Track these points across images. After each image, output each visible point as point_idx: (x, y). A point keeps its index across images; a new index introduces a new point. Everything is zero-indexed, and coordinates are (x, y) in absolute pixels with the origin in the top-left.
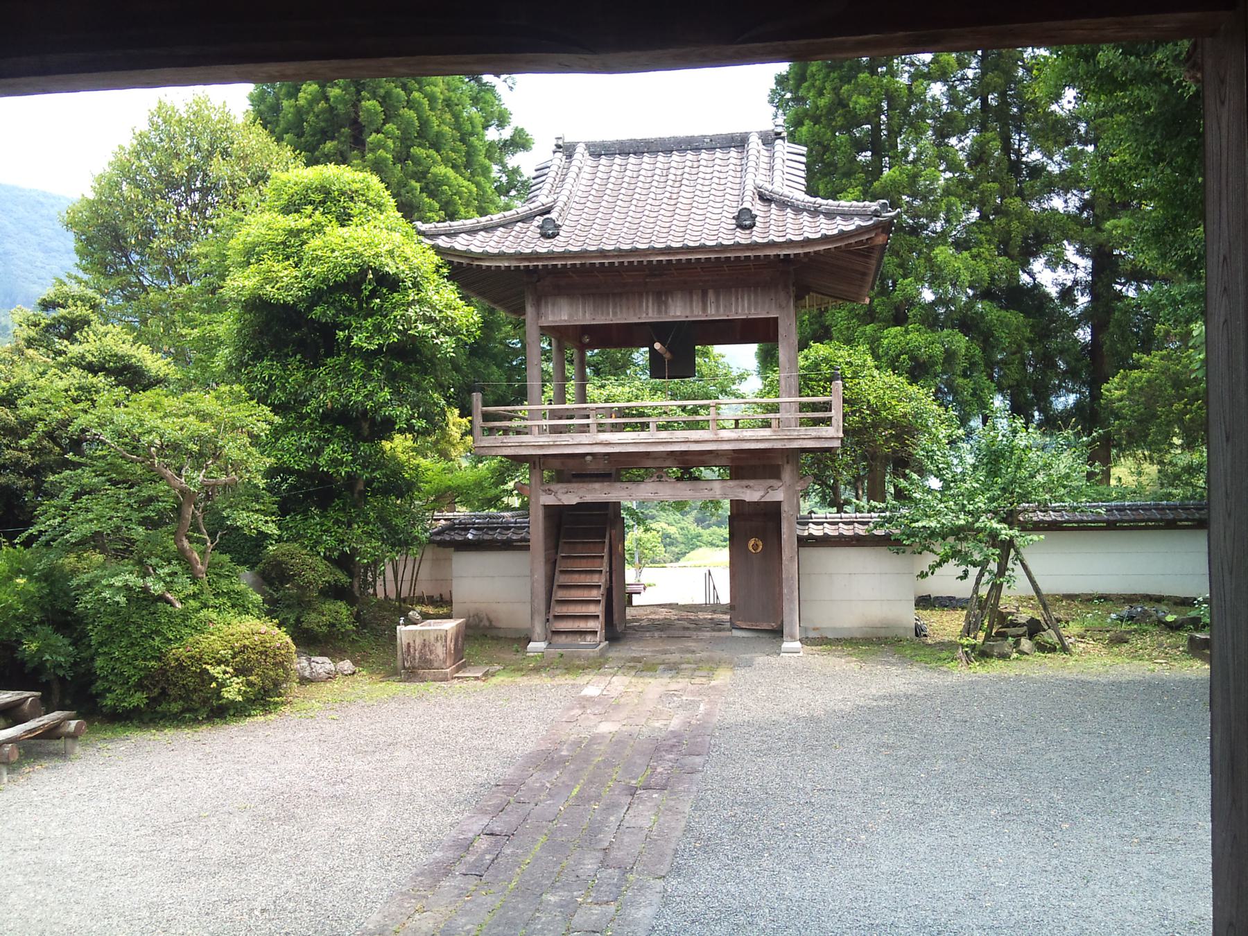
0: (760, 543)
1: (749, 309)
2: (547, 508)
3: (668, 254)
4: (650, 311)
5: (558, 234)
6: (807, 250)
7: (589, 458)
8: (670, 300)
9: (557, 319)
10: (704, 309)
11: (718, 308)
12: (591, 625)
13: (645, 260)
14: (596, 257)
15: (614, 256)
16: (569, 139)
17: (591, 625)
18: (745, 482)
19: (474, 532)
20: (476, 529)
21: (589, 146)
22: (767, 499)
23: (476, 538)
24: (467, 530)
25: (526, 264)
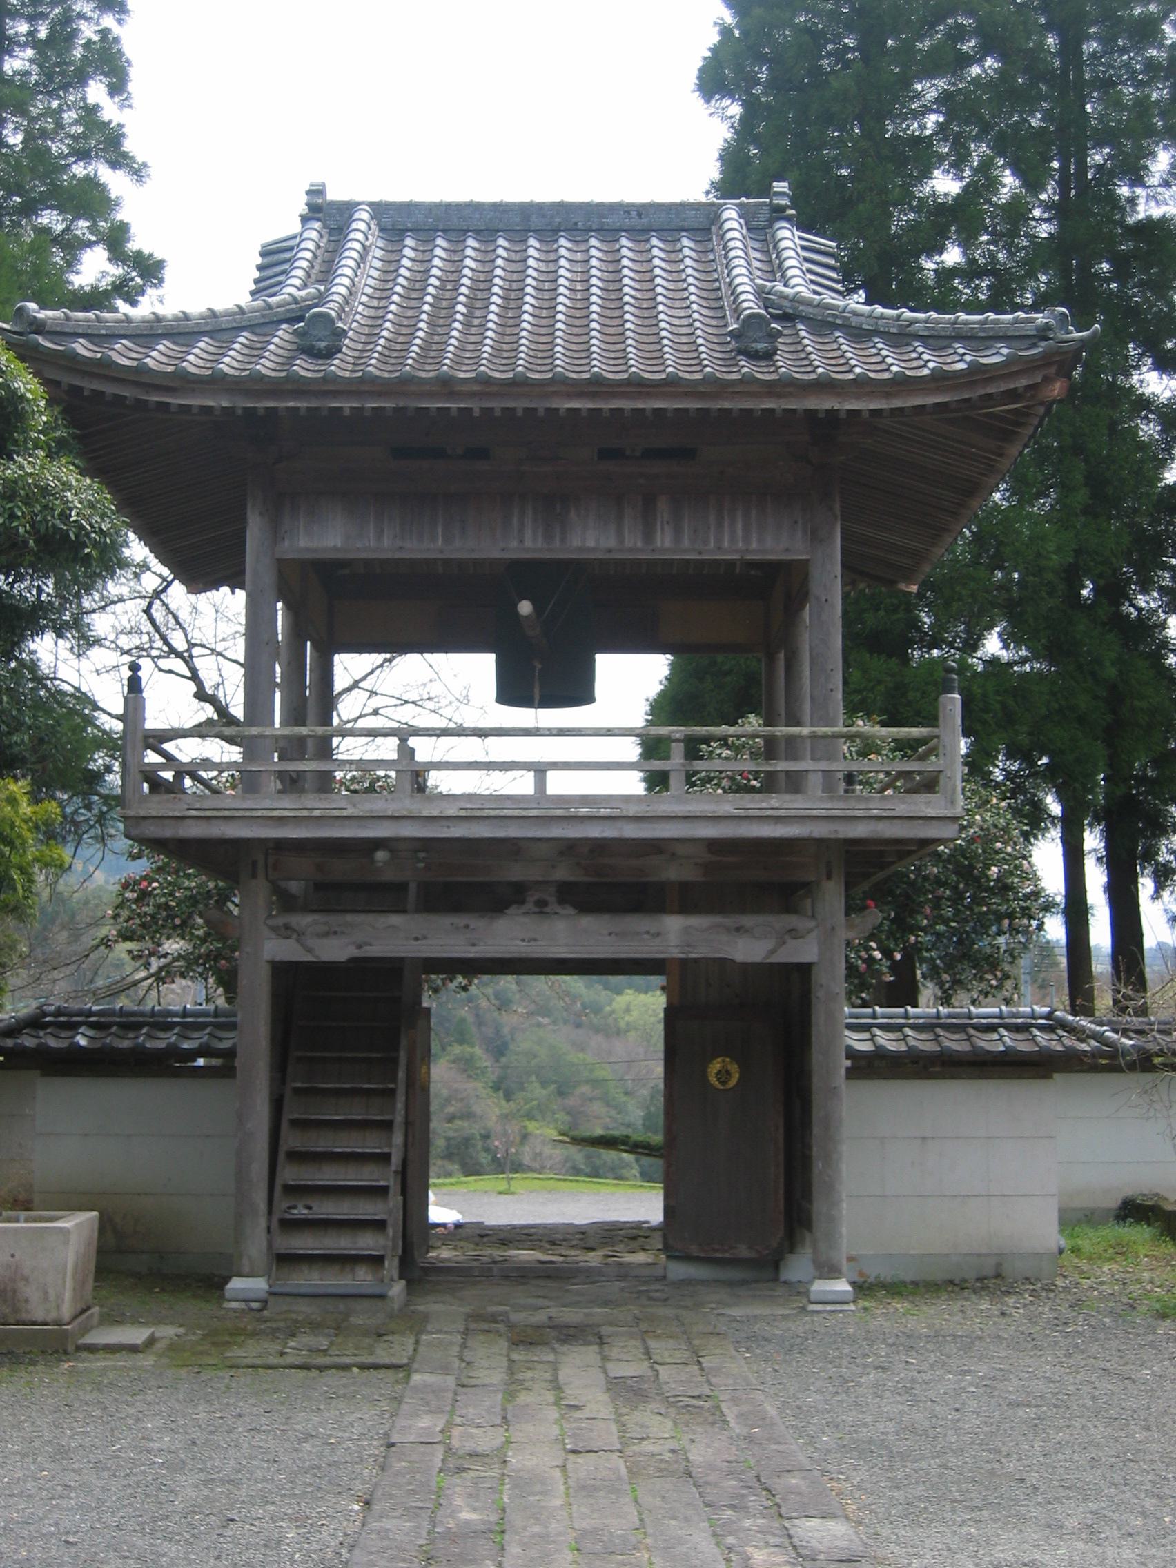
0: (734, 1069)
1: (746, 539)
2: (283, 972)
3: (593, 395)
4: (528, 534)
5: (339, 351)
6: (897, 403)
7: (381, 855)
8: (573, 514)
9: (315, 544)
10: (648, 536)
11: (678, 531)
12: (367, 1243)
13: (541, 405)
14: (432, 395)
15: (472, 395)
16: (335, 194)
17: (367, 1243)
18: (729, 921)
19: (91, 1033)
20: (92, 1026)
21: (379, 210)
22: (783, 956)
23: (98, 1045)
24: (73, 1027)
25: (271, 404)
